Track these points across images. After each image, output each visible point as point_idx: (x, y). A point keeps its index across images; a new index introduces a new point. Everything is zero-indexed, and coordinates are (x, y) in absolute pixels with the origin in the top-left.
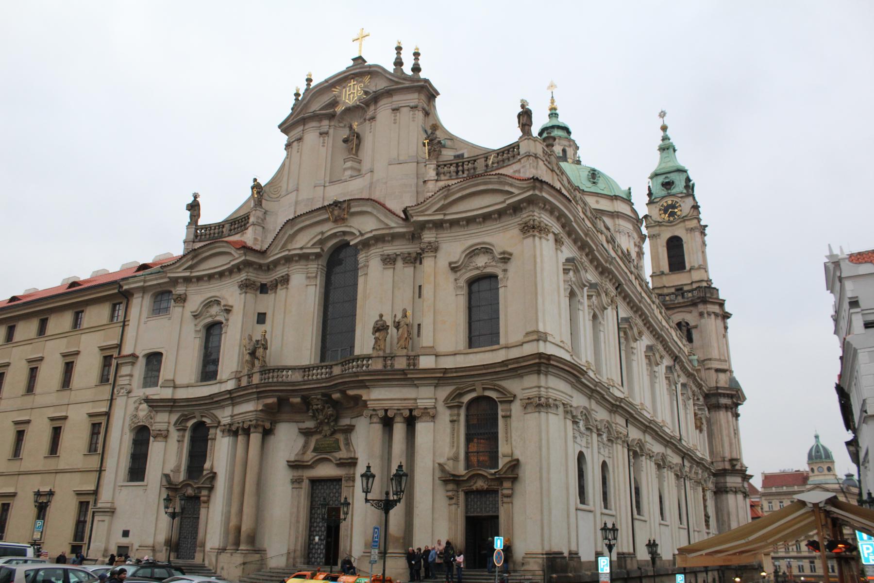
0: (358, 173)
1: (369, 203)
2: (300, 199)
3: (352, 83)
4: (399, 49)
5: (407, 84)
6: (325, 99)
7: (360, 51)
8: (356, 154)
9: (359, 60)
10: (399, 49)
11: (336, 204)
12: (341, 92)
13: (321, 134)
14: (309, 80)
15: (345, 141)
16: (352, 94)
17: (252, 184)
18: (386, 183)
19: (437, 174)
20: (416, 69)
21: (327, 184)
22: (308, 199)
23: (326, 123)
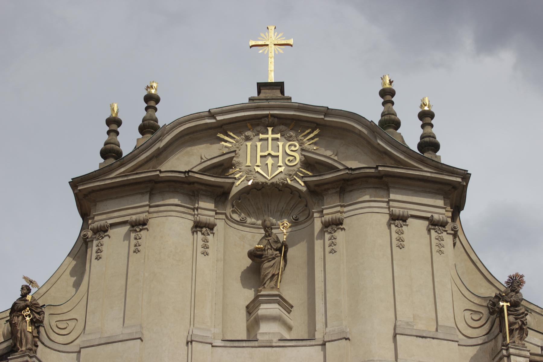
3: (270, 136)
4: (387, 94)
5: (427, 173)
10: (387, 94)
13: (198, 226)
14: (151, 100)
16: (271, 158)
20: (429, 145)
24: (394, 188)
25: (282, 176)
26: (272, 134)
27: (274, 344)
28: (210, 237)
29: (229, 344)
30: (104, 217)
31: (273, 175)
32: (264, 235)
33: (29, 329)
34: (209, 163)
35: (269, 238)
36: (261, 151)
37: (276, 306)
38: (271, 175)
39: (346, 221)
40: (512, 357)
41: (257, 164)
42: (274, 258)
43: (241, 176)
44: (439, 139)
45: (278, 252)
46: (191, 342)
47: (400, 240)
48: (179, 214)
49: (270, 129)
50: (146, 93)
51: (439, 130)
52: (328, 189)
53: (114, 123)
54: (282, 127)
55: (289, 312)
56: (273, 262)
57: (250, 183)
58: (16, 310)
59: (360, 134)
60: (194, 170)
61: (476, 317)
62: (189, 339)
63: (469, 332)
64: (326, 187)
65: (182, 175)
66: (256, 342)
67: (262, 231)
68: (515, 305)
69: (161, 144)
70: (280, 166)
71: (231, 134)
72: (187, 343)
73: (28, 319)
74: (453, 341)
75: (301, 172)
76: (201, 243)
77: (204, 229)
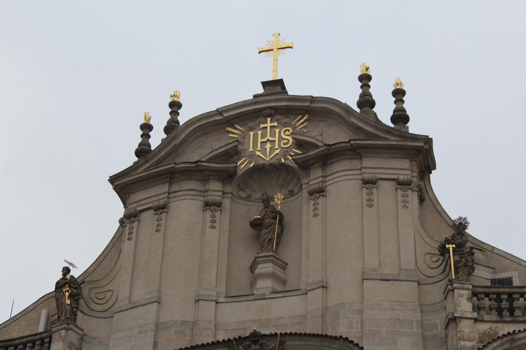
0: (284, 289)
3: (269, 125)
4: (365, 79)
5: (393, 141)
6: (215, 144)
7: (275, 71)
8: (276, 251)
9: (275, 86)
10: (365, 79)
12: (245, 135)
13: (207, 205)
15: (256, 225)
16: (270, 143)
17: (60, 276)
18: (361, 312)
19: (477, 309)
20: (400, 117)
22: (183, 322)
23: (215, 186)
24: (366, 157)
25: (278, 157)
26: (271, 123)
27: (267, 297)
28: (218, 214)
29: (230, 300)
30: (135, 205)
31: (271, 157)
32: (263, 207)
33: (68, 302)
34: (216, 153)
35: (267, 209)
36: (261, 138)
37: (271, 265)
39: (328, 188)
40: (456, 291)
41: (258, 149)
42: (270, 226)
43: (245, 161)
44: (408, 113)
45: (274, 220)
46: (199, 301)
48: (192, 197)
49: (269, 119)
51: (409, 105)
52: (314, 164)
53: (147, 128)
54: (278, 117)
57: (252, 165)
58: (59, 286)
59: (338, 115)
60: (203, 160)
61: (435, 259)
62: (197, 299)
63: (429, 272)
64: (311, 162)
65: (194, 165)
66: (252, 296)
68: (459, 247)
69: (176, 142)
70: (277, 149)
71: (238, 127)
73: (67, 294)
74: (413, 281)
75: (293, 152)
76: (209, 219)
77: (212, 207)
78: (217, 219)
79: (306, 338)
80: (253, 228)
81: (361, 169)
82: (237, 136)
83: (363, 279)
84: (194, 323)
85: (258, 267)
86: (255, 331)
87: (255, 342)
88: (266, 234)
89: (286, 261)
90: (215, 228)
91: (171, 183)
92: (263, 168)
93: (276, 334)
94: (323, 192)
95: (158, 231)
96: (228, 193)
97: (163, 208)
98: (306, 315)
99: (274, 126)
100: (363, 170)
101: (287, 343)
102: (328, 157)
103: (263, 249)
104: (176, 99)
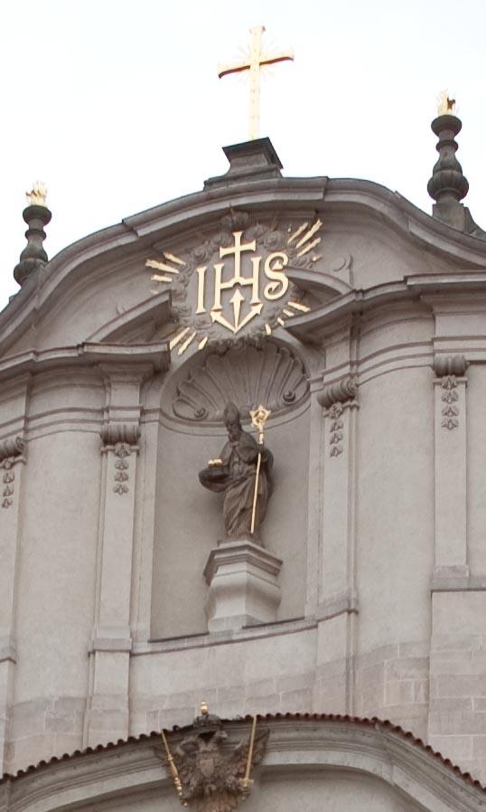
0: (274, 615)
1: (368, 737)
2: (24, 696)
3: (237, 248)
8: (258, 536)
11: (207, 729)
12: (186, 277)
13: (108, 440)
14: (37, 217)
15: (214, 479)
16: (240, 291)
18: (426, 662)
21: (143, 647)
22: (64, 699)
25: (259, 322)
26: (242, 243)
27: (235, 637)
28: (131, 460)
29: (159, 647)
32: (228, 439)
35: (236, 443)
36: (222, 282)
37: (244, 566)
38: (239, 324)
39: (363, 389)
42: (243, 479)
43: (188, 335)
45: (251, 467)
46: (94, 652)
47: (450, 412)
48: (75, 426)
50: (26, 203)
54: (258, 228)
55: (275, 573)
56: (243, 485)
57: (201, 346)
59: (383, 218)
60: (94, 340)
62: (90, 649)
65: (74, 354)
66: (205, 637)
67: (224, 431)
69: (35, 304)
70: (256, 304)
71: (170, 257)
72: (89, 654)
75: (291, 309)
77: (119, 446)
78: (131, 472)
79: (310, 724)
80: (209, 487)
81: (431, 343)
82: (169, 280)
83: (432, 591)
84: (86, 702)
85: (219, 572)
86: (205, 713)
87: (207, 737)
88: (234, 498)
89: (278, 557)
90: (125, 491)
91: (30, 397)
92: (228, 349)
93: (249, 719)
94: (352, 398)
95: (6, 504)
96: (154, 411)
97: (17, 454)
98: (314, 673)
99: (250, 252)
100: (437, 345)
101: (273, 736)
102: (361, 318)
103: (230, 532)
104: (39, 202)
